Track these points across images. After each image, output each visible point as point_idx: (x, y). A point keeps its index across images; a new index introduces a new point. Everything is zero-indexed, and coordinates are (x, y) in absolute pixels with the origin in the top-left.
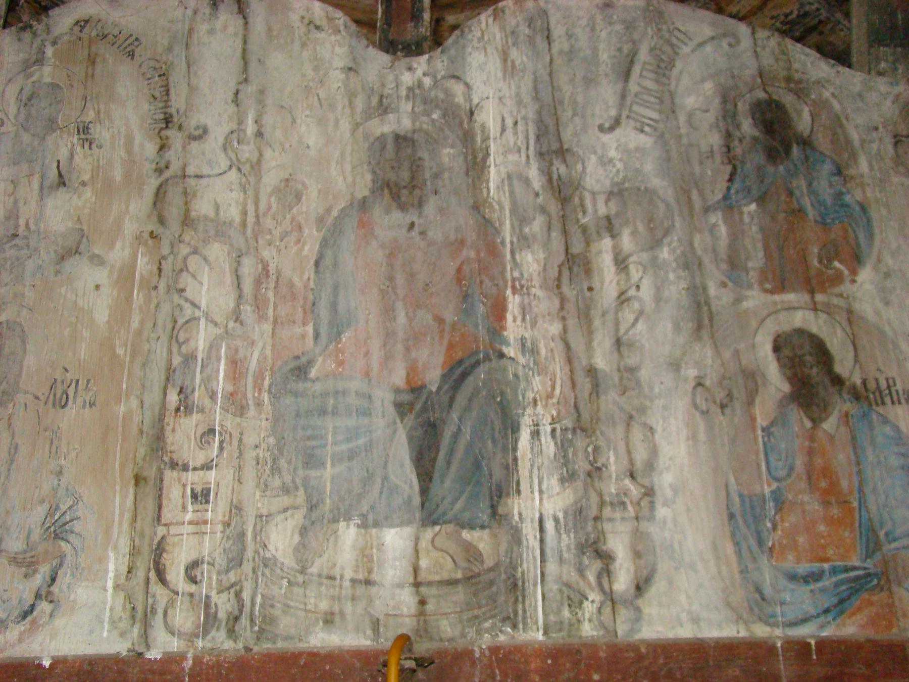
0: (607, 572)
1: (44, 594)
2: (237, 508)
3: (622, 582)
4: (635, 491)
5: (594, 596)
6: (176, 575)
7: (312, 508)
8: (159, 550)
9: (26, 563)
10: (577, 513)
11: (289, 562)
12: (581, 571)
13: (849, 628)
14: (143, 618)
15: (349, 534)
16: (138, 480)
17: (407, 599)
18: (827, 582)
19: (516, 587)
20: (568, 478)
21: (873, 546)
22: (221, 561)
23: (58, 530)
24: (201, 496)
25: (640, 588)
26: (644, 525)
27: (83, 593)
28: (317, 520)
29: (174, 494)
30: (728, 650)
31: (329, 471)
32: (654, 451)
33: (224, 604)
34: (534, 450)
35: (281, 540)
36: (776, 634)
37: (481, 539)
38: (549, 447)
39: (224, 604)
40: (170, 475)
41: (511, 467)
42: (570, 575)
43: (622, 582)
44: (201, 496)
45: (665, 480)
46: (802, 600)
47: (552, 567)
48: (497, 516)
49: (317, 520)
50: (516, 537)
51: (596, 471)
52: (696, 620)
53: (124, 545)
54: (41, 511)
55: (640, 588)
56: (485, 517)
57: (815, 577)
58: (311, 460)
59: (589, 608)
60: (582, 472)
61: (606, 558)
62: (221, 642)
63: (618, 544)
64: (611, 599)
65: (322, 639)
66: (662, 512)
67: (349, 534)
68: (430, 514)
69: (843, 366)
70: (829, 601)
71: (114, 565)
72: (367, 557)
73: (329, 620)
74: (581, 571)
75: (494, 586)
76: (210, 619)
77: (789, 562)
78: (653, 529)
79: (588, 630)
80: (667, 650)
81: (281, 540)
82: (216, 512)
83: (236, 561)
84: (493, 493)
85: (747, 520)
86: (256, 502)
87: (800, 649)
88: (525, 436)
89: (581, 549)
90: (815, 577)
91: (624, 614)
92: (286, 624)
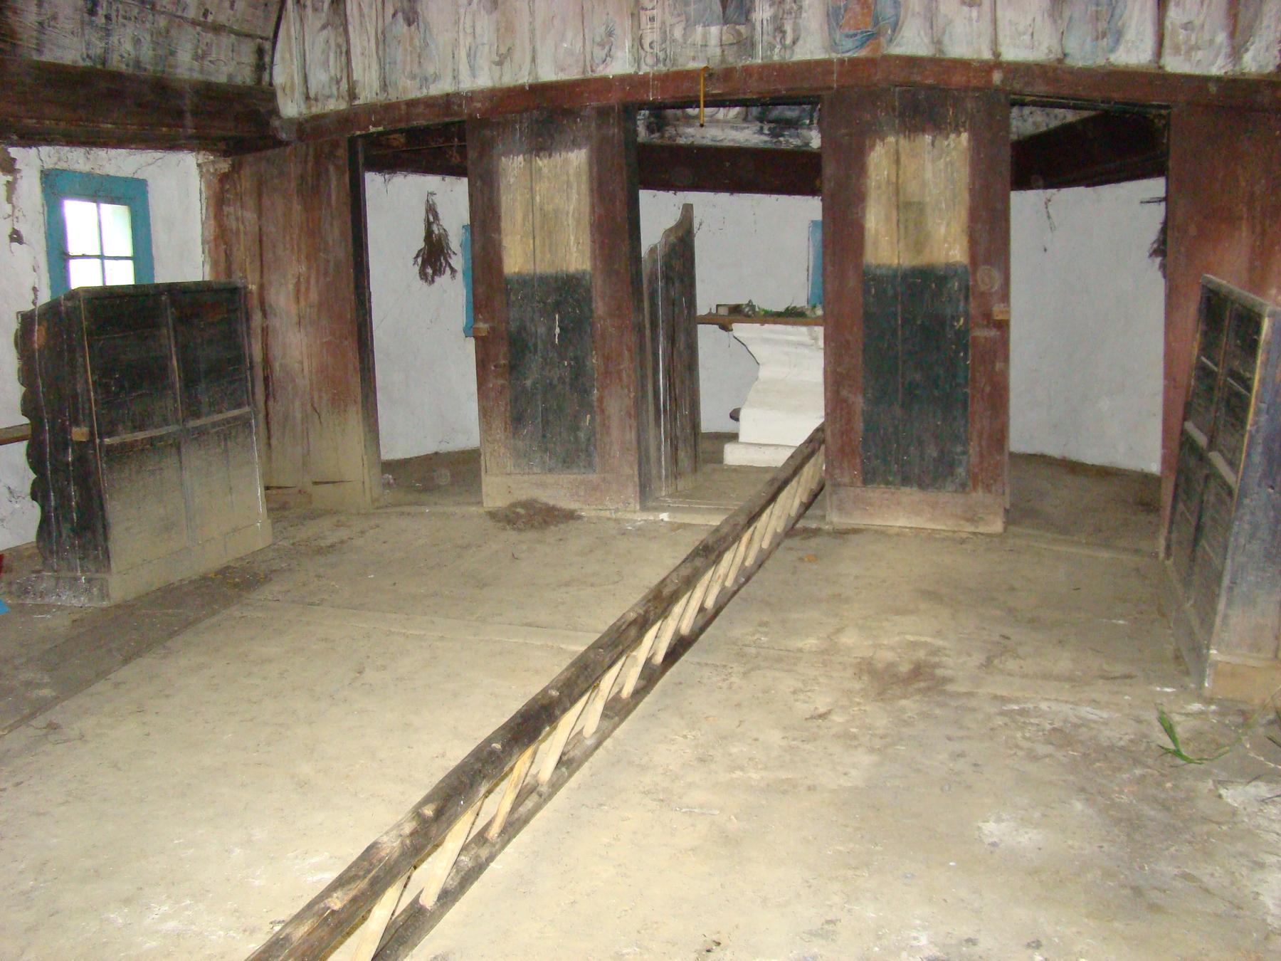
0: (784, 37)
1: (609, 55)
2: (663, 23)
3: (788, 41)
4: (795, 7)
5: (779, 46)
6: (646, 46)
8: (641, 38)
9: (602, 45)
10: (775, 17)
11: (681, 40)
12: (775, 37)
13: (863, 53)
14: (638, 61)
15: (699, 29)
16: (632, 15)
17: (718, 51)
18: (859, 37)
19: (753, 45)
21: (876, 23)
22: (660, 41)
24: (652, 19)
25: (794, 43)
26: (800, 21)
28: (689, 25)
29: (644, 19)
30: (818, 63)
31: (693, 7)
33: (661, 55)
35: (678, 33)
36: (834, 56)
37: (742, 28)
39: (661, 55)
40: (642, 13)
42: (771, 39)
43: (788, 41)
44: (652, 19)
46: (849, 44)
47: (765, 37)
48: (748, 20)
49: (689, 25)
52: (812, 52)
53: (630, 36)
54: (603, 28)
55: (794, 43)
56: (743, 20)
57: (855, 35)
59: (777, 50)
61: (784, 32)
62: (662, 68)
63: (788, 28)
64: (784, 47)
65: (692, 65)
66: (804, 15)
67: (699, 29)
68: (726, 21)
70: (857, 43)
71: (628, 44)
72: (705, 37)
73: (694, 58)
74: (775, 37)
75: (746, 45)
76: (658, 61)
77: (846, 31)
78: (800, 21)
79: (776, 58)
81: (678, 33)
82: (657, 24)
83: (664, 41)
86: (670, 20)
87: (842, 62)
89: (775, 30)
90: (855, 35)
91: (788, 52)
92: (681, 61)
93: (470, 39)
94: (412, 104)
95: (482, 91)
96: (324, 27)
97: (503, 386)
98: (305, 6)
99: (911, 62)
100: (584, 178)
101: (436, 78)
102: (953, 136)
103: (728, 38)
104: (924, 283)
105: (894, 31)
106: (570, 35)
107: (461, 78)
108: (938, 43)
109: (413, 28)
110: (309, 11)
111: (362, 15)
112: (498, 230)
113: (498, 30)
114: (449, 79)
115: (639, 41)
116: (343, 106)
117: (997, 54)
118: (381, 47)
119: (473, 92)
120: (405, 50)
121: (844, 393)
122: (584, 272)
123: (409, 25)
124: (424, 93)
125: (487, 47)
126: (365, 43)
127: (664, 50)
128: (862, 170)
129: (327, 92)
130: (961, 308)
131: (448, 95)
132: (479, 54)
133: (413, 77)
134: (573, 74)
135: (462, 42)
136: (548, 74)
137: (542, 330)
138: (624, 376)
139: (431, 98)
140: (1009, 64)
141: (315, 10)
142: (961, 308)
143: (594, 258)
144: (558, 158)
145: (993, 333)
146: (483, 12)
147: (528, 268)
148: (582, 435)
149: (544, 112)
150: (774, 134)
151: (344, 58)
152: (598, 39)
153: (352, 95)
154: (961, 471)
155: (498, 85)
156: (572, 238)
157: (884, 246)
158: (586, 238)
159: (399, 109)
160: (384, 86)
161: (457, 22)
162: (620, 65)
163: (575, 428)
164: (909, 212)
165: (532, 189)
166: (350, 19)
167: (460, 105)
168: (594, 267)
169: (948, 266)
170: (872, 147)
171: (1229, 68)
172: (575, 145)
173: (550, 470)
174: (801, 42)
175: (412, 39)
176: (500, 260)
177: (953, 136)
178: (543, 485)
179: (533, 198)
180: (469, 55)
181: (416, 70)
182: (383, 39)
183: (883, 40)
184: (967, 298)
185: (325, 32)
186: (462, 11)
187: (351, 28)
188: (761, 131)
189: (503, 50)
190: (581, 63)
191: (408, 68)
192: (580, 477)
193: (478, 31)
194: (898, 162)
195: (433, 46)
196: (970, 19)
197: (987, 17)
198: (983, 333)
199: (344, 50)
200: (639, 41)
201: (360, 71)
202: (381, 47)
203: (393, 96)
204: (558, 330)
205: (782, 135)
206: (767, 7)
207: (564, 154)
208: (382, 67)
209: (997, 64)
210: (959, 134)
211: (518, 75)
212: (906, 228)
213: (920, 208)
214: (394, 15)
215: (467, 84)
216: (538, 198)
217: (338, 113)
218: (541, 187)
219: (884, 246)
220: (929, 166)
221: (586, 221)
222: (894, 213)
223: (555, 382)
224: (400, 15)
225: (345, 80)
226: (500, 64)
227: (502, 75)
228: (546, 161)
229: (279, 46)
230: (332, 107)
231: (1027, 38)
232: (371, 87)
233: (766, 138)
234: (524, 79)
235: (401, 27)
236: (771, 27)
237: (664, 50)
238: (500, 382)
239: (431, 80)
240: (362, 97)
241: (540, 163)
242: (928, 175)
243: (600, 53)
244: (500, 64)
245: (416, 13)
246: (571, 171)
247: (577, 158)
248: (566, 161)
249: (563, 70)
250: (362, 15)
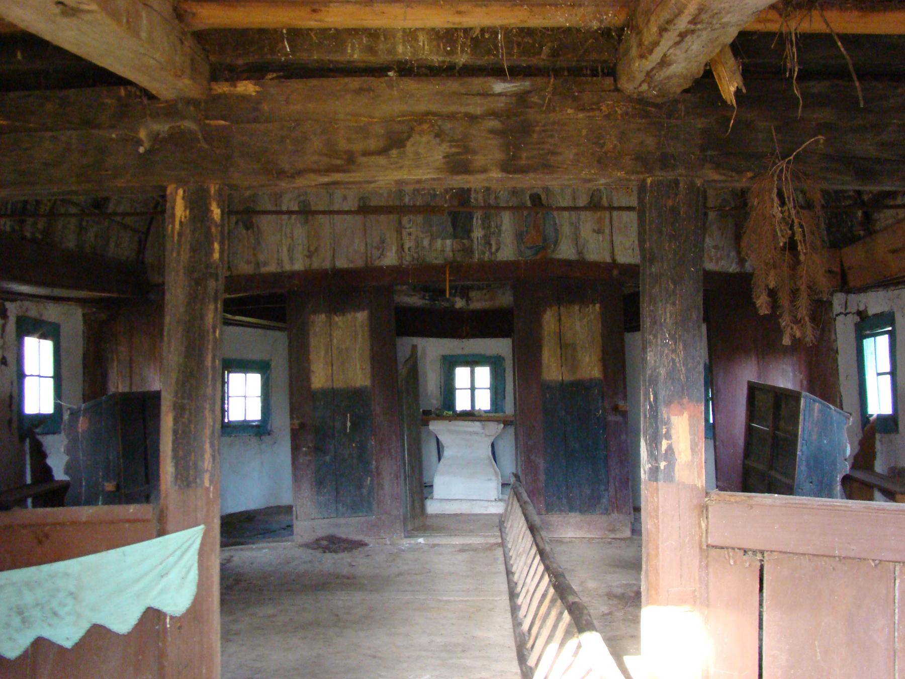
1: (382, 254)
2: (417, 236)
3: (493, 250)
6: (406, 250)
7: (432, 235)
8: (402, 245)
9: (378, 249)
10: (485, 236)
15: (439, 241)
17: (451, 254)
20: (483, 228)
21: (545, 240)
23: (383, 241)
24: (410, 234)
27: (389, 254)
28: (433, 239)
29: (404, 233)
32: (502, 222)
34: (477, 222)
35: (426, 243)
37: (465, 241)
38: (480, 222)
41: (472, 225)
43: (493, 250)
45: (504, 228)
46: (529, 252)
48: (469, 238)
49: (433, 239)
50: (472, 241)
51: (489, 227)
55: (497, 251)
58: (431, 226)
60: (486, 226)
61: (491, 245)
63: (493, 242)
64: (491, 253)
65: (435, 262)
67: (439, 241)
68: (455, 236)
69: (544, 201)
71: (394, 249)
72: (443, 246)
73: (436, 259)
75: (469, 251)
80: (501, 262)
82: (413, 237)
83: (417, 247)
84: (468, 232)
85: (520, 236)
86: (421, 235)
88: (475, 220)
93: (289, 240)
97: (310, 461)
99: (567, 263)
100: (366, 329)
101: (266, 264)
102: (591, 306)
103: (457, 246)
104: (576, 390)
105: (555, 245)
106: (357, 241)
108: (580, 253)
112: (308, 360)
113: (308, 236)
115: (401, 247)
117: (614, 260)
121: (533, 457)
122: (366, 387)
123: (247, 229)
125: (300, 247)
127: (418, 253)
128: (540, 326)
130: (600, 405)
133: (249, 263)
134: (360, 263)
135: (284, 242)
136: (342, 264)
137: (338, 424)
138: (393, 451)
140: (622, 265)
142: (600, 405)
143: (373, 377)
144: (349, 316)
145: (619, 418)
147: (329, 385)
148: (365, 491)
149: (339, 288)
150: (431, 299)
152: (375, 245)
154: (604, 501)
156: (358, 367)
157: (553, 370)
158: (368, 366)
162: (390, 259)
163: (360, 486)
164: (567, 349)
165: (331, 335)
168: (373, 385)
169: (591, 380)
170: (545, 311)
171: (738, 270)
172: (360, 308)
173: (343, 515)
174: (501, 251)
176: (309, 380)
177: (591, 306)
178: (338, 526)
179: (331, 341)
180: (289, 251)
183: (549, 251)
184: (602, 397)
188: (423, 298)
189: (312, 249)
190: (364, 258)
192: (363, 519)
193: (296, 236)
194: (560, 320)
196: (598, 240)
197: (608, 238)
198: (612, 418)
200: (401, 247)
204: (349, 424)
205: (438, 300)
206: (480, 230)
207: (353, 314)
209: (614, 264)
210: (594, 305)
211: (322, 262)
212: (566, 360)
213: (574, 347)
215: (288, 267)
216: (335, 341)
218: (337, 334)
219: (553, 370)
220: (578, 323)
221: (367, 354)
222: (559, 350)
223: (346, 456)
224: (240, 223)
226: (310, 257)
228: (341, 318)
229: (150, 238)
231: (630, 251)
233: (427, 302)
234: (327, 265)
236: (483, 242)
237: (418, 253)
238: (308, 458)
241: (337, 319)
242: (578, 328)
243: (377, 253)
244: (310, 257)
246: (358, 324)
247: (362, 316)
248: (355, 319)
249: (352, 262)
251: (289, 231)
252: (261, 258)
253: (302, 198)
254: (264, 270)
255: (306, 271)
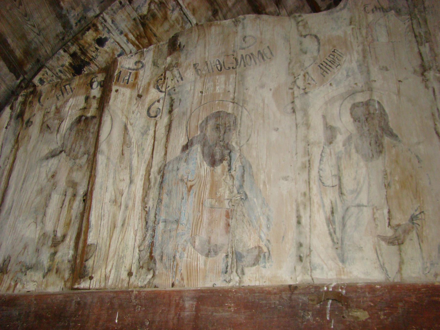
93: (331, 196)
94: (205, 297)
95: (371, 288)
96: (53, 155)
98: (29, 123)
101: (260, 256)
107: (315, 259)
109: (219, 169)
110: (34, 130)
111: (126, 142)
113: (388, 186)
114: (290, 261)
116: (55, 286)
118: (153, 193)
119: (352, 288)
120: (201, 203)
123: (213, 163)
124: (234, 281)
125: (367, 213)
126: (123, 186)
129: (28, 258)
131: (292, 289)
132: (351, 222)
133: (210, 251)
135: (316, 199)
139: (252, 290)
141: (46, 127)
146: (355, 156)
151: (77, 204)
153: (79, 271)
155: (394, 278)
159: (180, 308)
160: (149, 261)
161: (307, 166)
166: (103, 146)
167: (321, 313)
175: (214, 186)
180: (330, 222)
181: (220, 238)
182: (159, 180)
185: (54, 161)
186: (316, 151)
187: (101, 159)
189: (400, 219)
191: (203, 235)
193: (349, 184)
195: (255, 201)
199: (81, 191)
201: (105, 233)
202: (153, 193)
203: (164, 281)
208: (149, 225)
214: (186, 147)
215: (327, 272)
217: (41, 298)
224: (197, 148)
225: (70, 241)
226: (396, 241)
227: (401, 263)
230: (31, 287)
232: (121, 258)
235: (197, 165)
239: (249, 259)
240: (96, 277)
245: (227, 147)
250: (126, 142)
251: (329, 170)
252: (248, 239)
253: (360, 98)
254: (255, 277)
255: (392, 288)
